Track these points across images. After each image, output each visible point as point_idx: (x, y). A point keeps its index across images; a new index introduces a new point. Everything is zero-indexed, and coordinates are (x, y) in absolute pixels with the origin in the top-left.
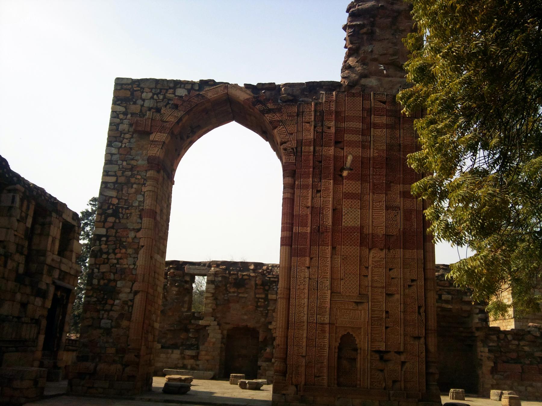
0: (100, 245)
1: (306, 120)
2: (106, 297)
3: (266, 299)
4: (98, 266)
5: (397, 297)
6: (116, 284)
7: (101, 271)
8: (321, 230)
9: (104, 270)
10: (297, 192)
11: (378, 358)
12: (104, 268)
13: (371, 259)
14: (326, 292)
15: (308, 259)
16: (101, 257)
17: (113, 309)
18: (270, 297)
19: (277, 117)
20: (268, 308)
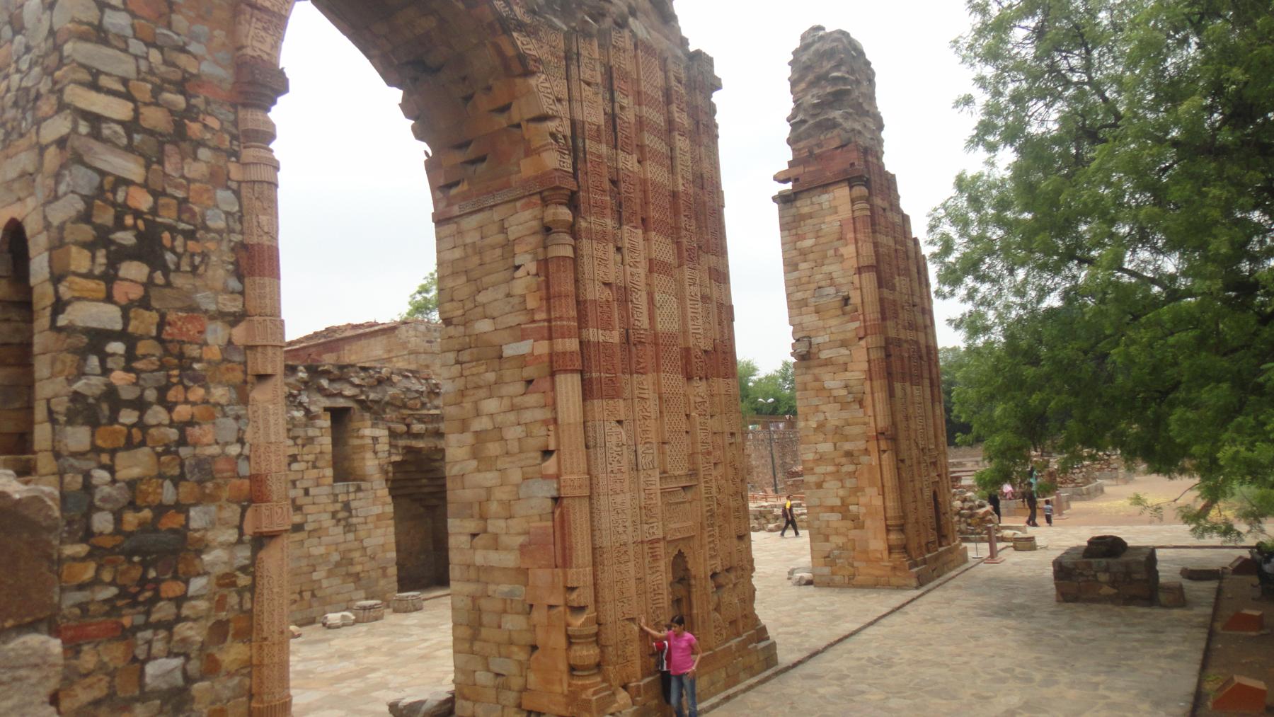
0: (106, 371)
2: (152, 574)
4: (105, 458)
6: (187, 519)
7: (125, 473)
9: (135, 472)
12: (134, 465)
16: (113, 419)
17: (185, 611)
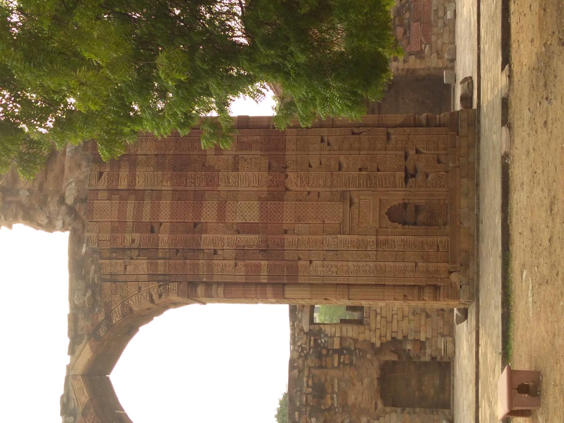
1: (122, 269)
3: (340, 352)
5: (342, 158)
8: (264, 248)
10: (216, 279)
11: (413, 179)
13: (298, 189)
14: (339, 240)
15: (300, 263)
18: (337, 346)
19: (117, 309)
20: (353, 348)
